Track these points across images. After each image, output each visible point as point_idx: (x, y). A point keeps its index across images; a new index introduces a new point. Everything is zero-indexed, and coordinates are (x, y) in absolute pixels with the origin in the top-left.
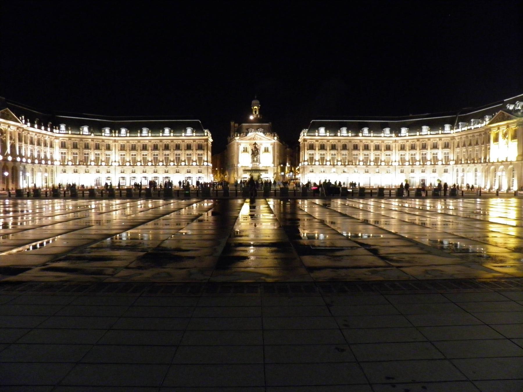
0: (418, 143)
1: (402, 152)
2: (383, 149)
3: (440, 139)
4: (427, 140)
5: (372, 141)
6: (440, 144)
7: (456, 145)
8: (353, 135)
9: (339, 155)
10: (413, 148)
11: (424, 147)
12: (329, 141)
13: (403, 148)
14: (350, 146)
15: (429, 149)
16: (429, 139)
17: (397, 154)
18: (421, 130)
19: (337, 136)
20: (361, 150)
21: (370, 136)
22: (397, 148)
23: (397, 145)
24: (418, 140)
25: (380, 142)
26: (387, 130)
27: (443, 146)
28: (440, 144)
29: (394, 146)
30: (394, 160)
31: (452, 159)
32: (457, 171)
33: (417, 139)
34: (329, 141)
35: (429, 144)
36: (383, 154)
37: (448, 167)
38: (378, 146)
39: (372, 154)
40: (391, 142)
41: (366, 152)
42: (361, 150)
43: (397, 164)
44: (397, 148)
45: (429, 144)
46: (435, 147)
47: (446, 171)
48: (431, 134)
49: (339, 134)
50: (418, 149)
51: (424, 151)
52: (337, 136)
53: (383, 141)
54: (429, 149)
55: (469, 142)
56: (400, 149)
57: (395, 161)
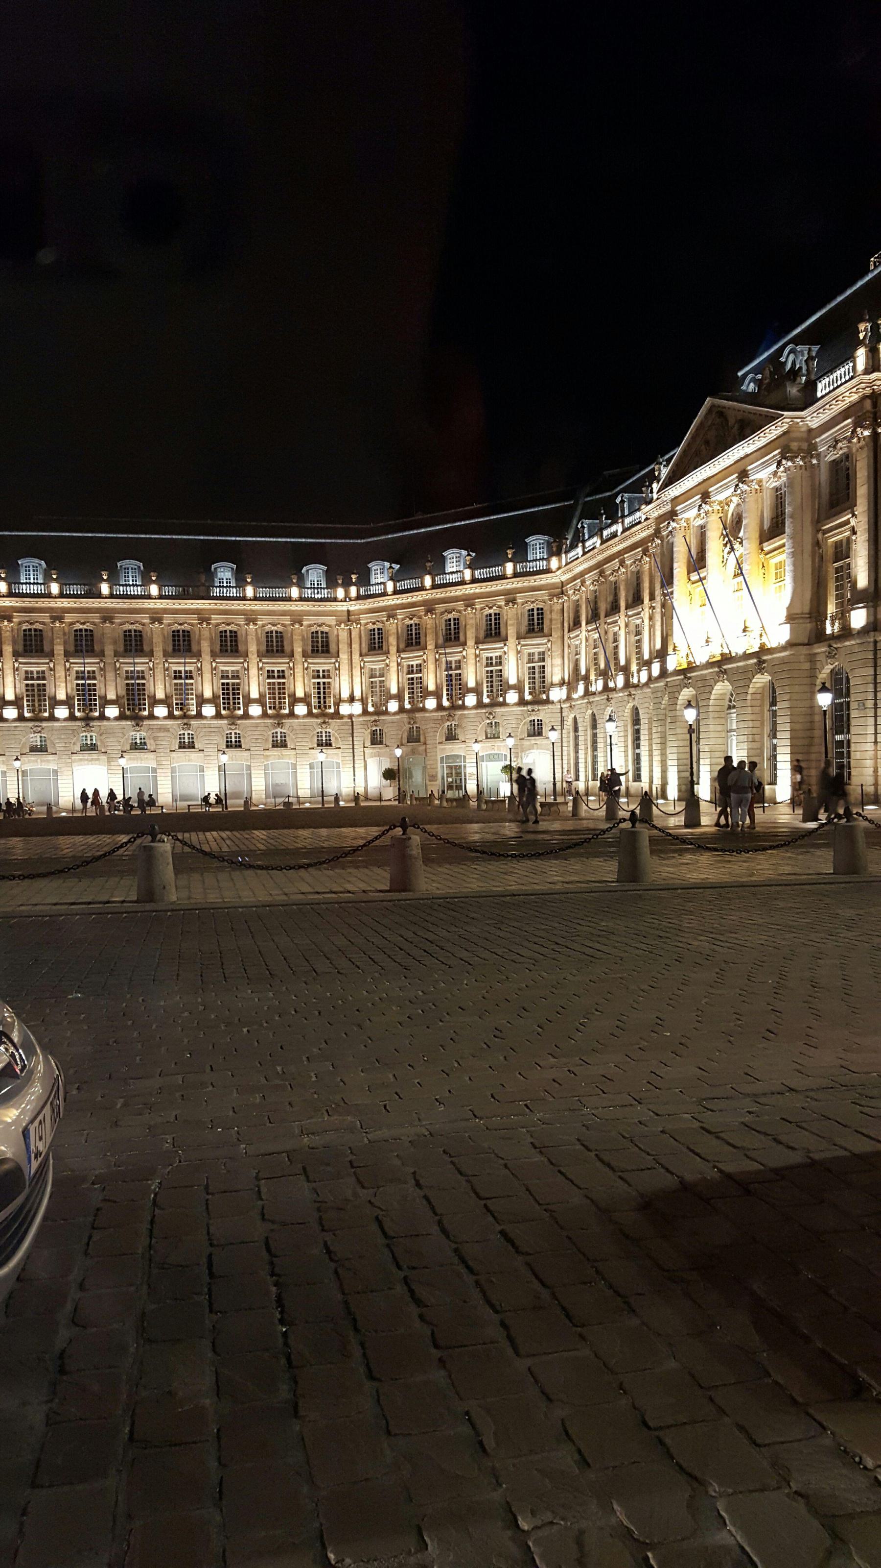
0: (428, 621)
1: (375, 663)
2: (298, 650)
3: (511, 598)
4: (460, 605)
5: (251, 618)
6: (513, 619)
7: (568, 616)
8: (168, 590)
9: (110, 675)
10: (413, 640)
11: (453, 635)
12: (60, 619)
13: (376, 644)
14: (157, 635)
15: (471, 642)
16: (469, 601)
17: (357, 672)
18: (439, 567)
19: (99, 596)
20: (206, 657)
21: (244, 598)
22: (356, 646)
23: (355, 634)
24: (429, 607)
25: (287, 620)
26: (315, 574)
27: (524, 629)
28: (513, 619)
29: (344, 636)
30: (345, 695)
31: (556, 679)
32: (576, 729)
33: (424, 603)
34: (60, 619)
35: (472, 621)
36: (299, 670)
37: (544, 714)
38: (280, 636)
39: (253, 672)
40: (331, 620)
41: (229, 666)
42: (206, 657)
43: (357, 709)
44: (356, 646)
45: (472, 621)
46: (493, 631)
47: (536, 730)
48: (474, 581)
49: (105, 589)
50: (431, 646)
51: (454, 654)
52: (99, 596)
53: (297, 618)
54: (471, 642)
55: (610, 598)
56: (365, 649)
57: (352, 699)
